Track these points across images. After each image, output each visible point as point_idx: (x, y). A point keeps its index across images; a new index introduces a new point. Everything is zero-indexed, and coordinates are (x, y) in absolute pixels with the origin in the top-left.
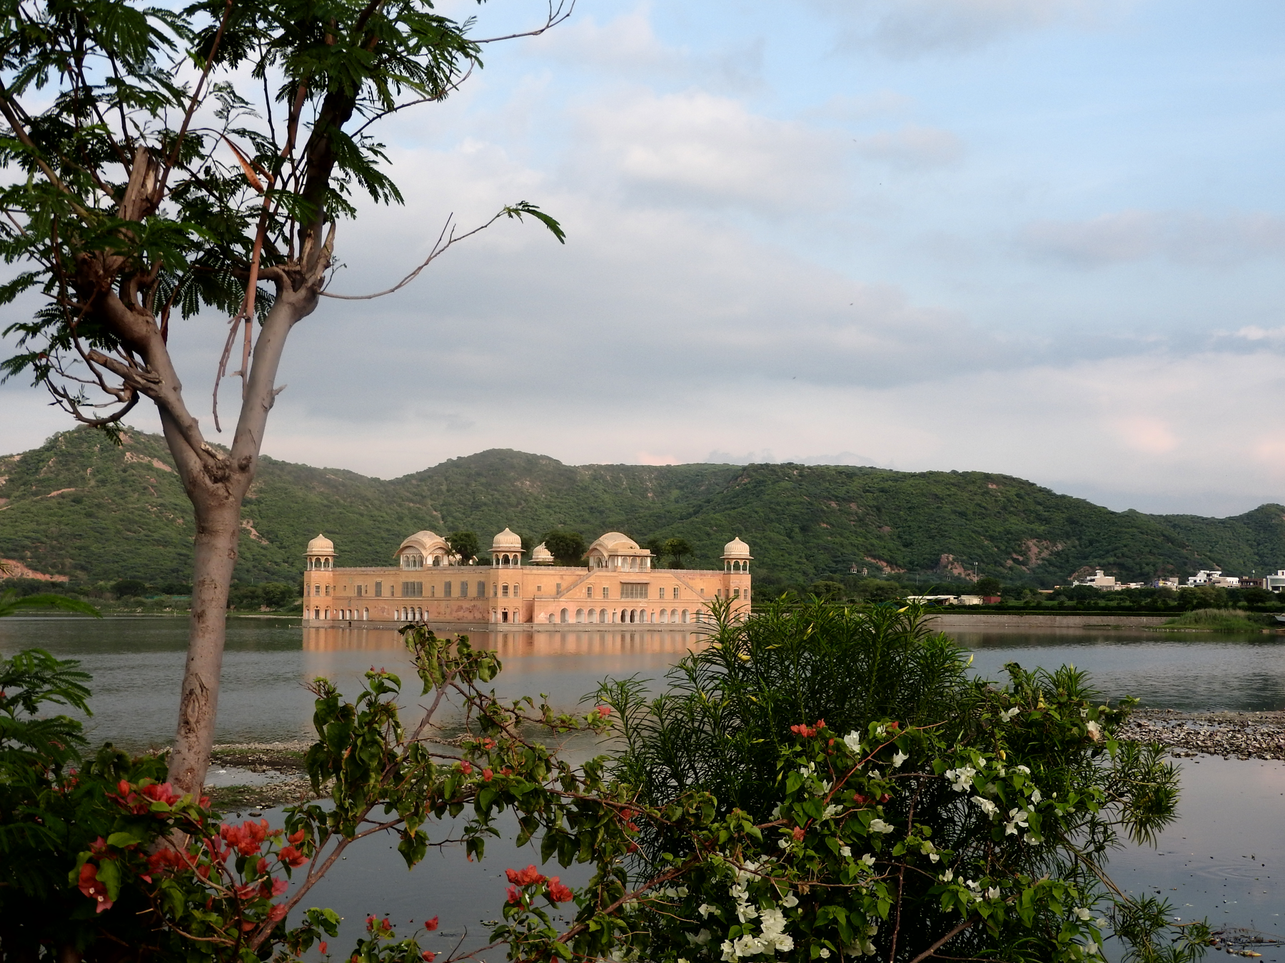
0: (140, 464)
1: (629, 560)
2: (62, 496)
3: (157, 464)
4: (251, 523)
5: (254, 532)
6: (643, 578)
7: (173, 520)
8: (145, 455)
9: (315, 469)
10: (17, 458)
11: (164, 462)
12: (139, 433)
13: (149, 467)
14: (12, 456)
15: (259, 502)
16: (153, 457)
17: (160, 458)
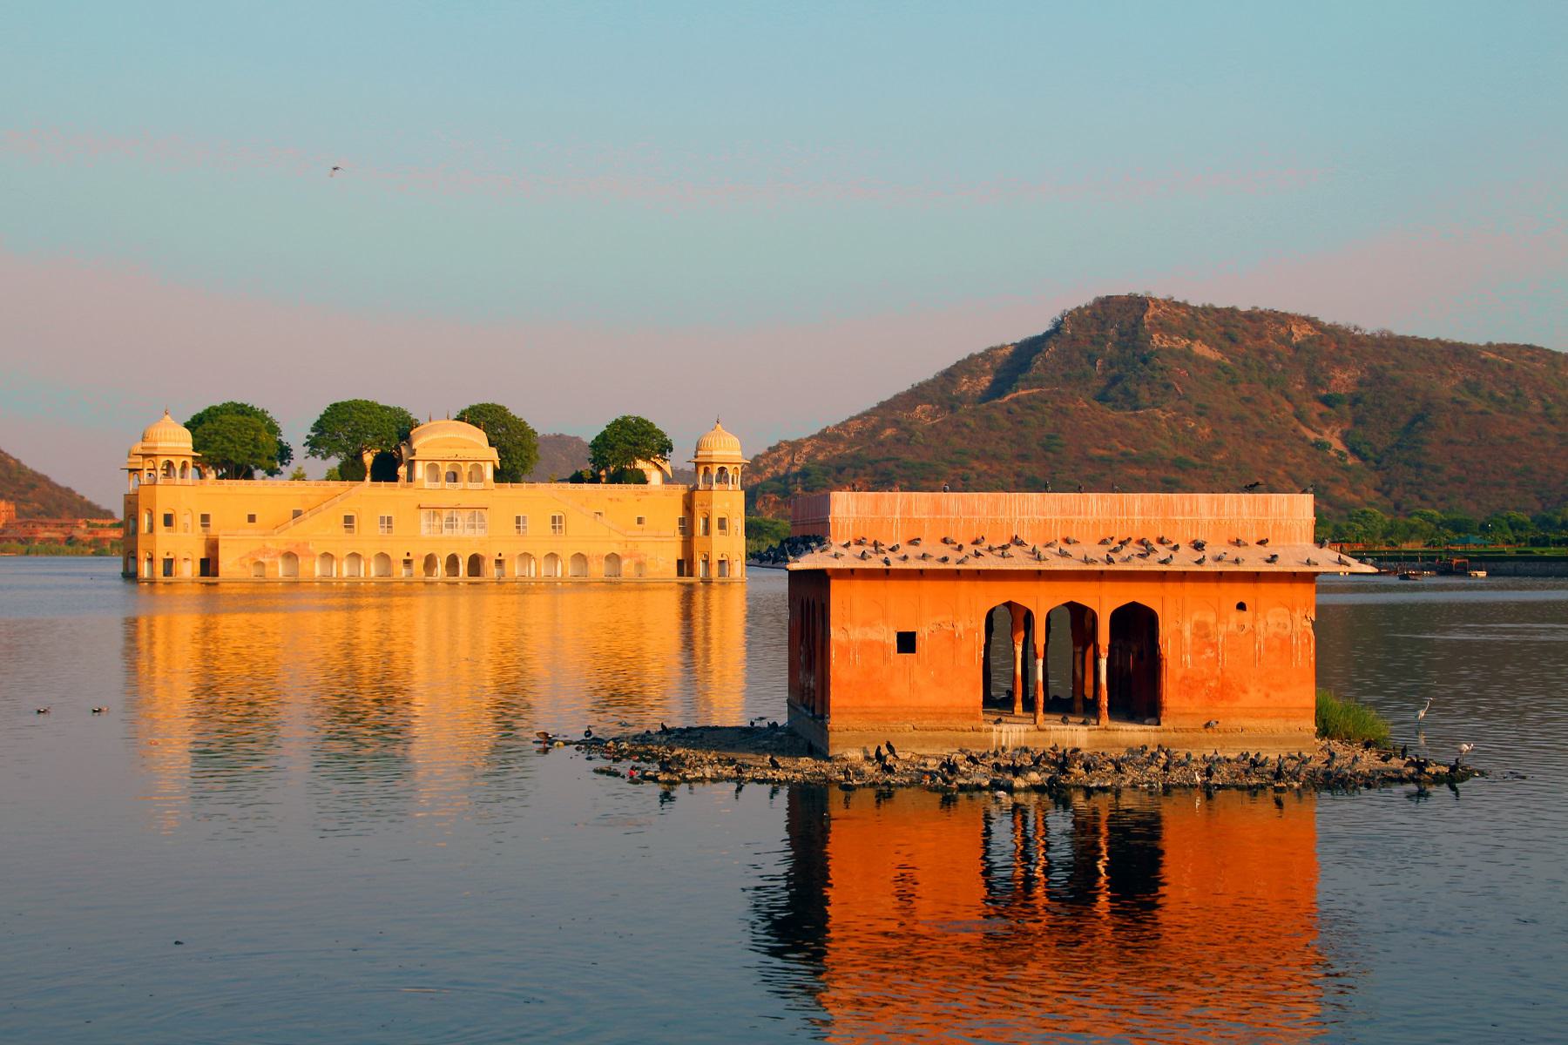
0: (1170, 351)
1: (445, 469)
2: (1017, 401)
3: (1200, 349)
4: (1337, 433)
5: (1337, 444)
6: (478, 500)
7: (1194, 431)
8: (1183, 336)
9: (1463, 346)
10: (1011, 349)
11: (1210, 347)
12: (1185, 306)
13: (1187, 355)
14: (1003, 347)
15: (1355, 401)
16: (1193, 338)
17: (1204, 341)
